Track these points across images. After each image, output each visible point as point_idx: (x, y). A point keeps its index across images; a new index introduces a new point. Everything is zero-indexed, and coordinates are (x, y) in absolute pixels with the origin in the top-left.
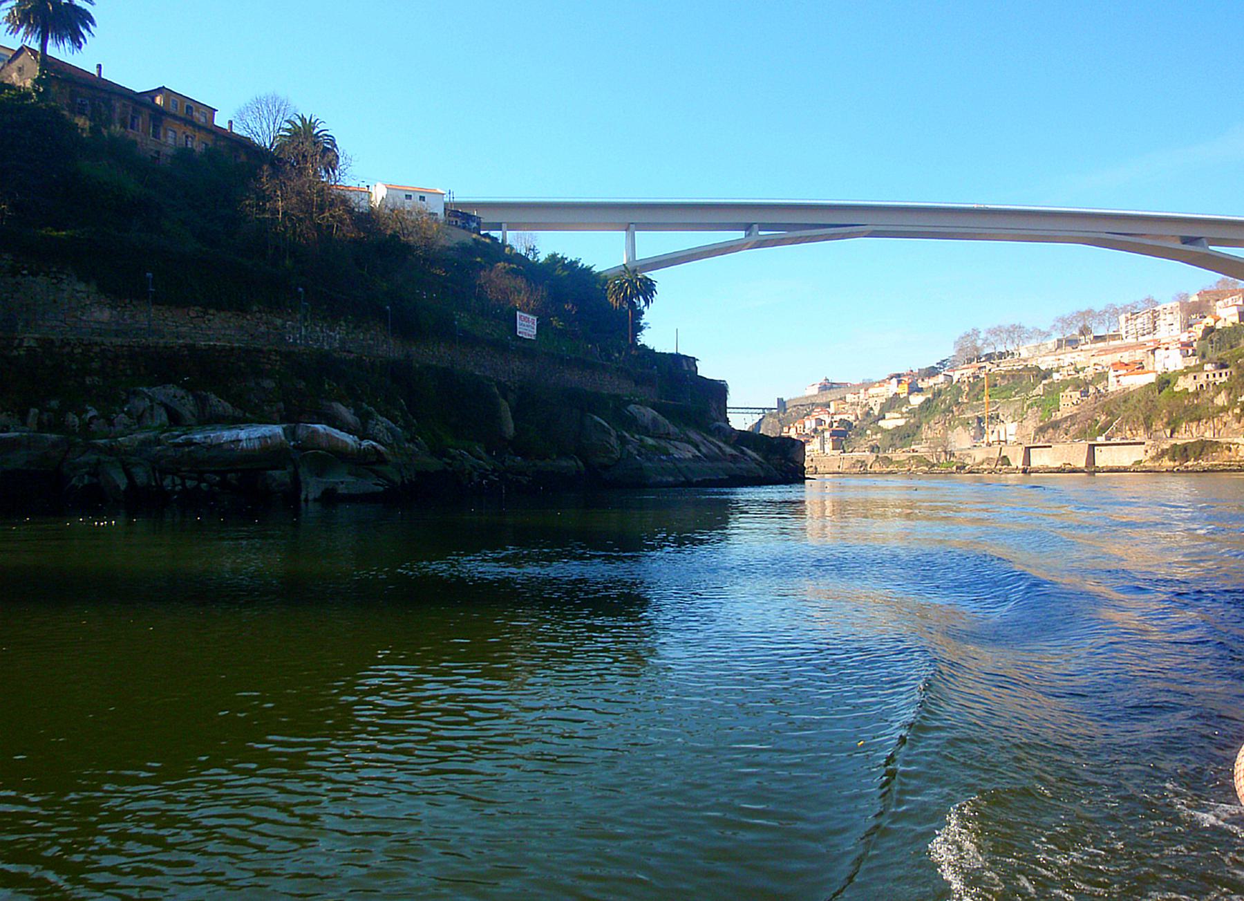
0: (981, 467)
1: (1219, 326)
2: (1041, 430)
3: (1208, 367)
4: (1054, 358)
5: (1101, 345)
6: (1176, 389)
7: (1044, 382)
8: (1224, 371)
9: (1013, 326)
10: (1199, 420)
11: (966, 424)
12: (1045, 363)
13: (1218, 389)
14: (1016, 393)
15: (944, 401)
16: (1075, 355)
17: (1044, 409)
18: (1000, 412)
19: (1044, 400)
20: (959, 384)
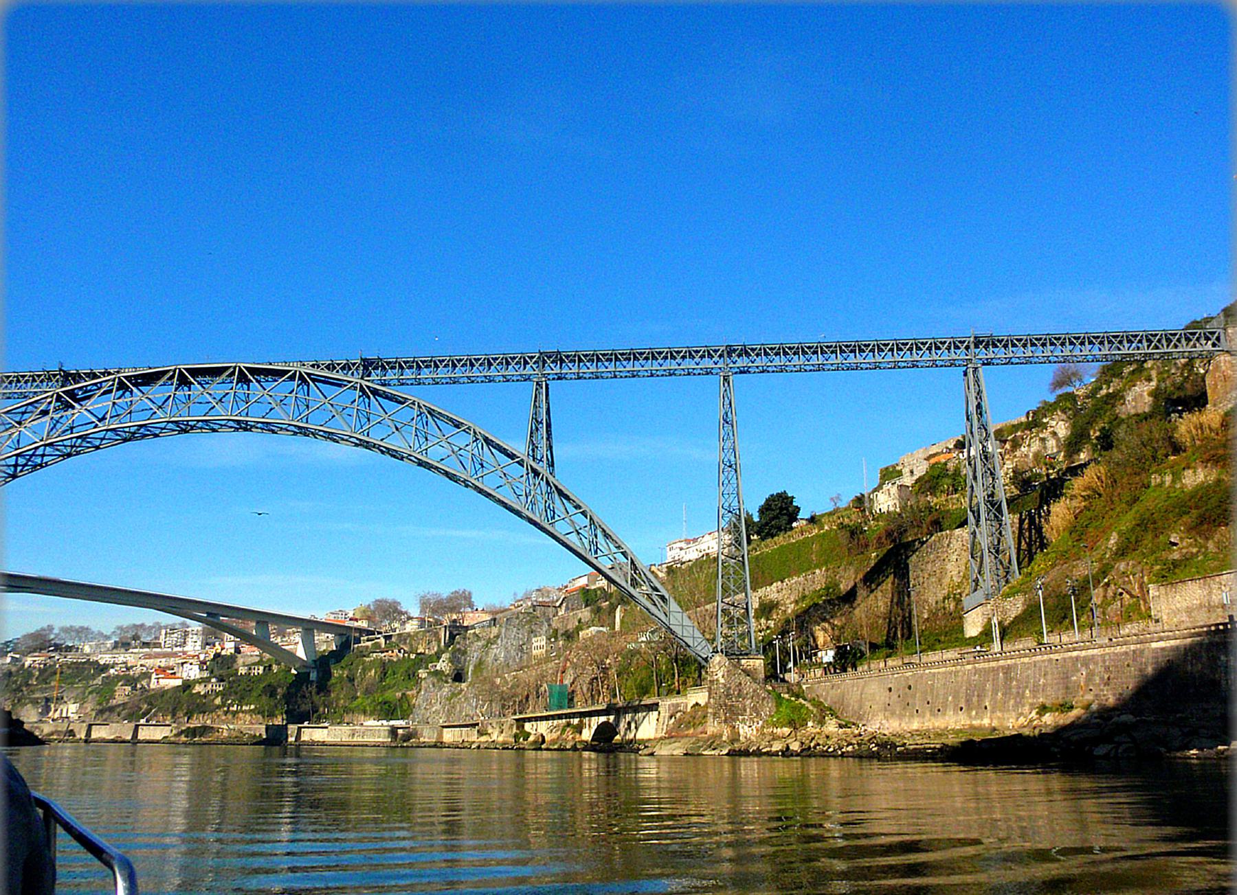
0: (52, 737)
1: (223, 653)
2: (101, 712)
3: (213, 680)
4: (111, 656)
5: (147, 650)
6: (194, 692)
7: (103, 675)
8: (222, 684)
9: (81, 627)
10: (205, 713)
11: (35, 702)
12: (104, 659)
13: (217, 694)
14: (80, 681)
15: (16, 681)
16: (126, 655)
17: (101, 696)
18: (65, 694)
19: (102, 689)
20: (30, 669)
